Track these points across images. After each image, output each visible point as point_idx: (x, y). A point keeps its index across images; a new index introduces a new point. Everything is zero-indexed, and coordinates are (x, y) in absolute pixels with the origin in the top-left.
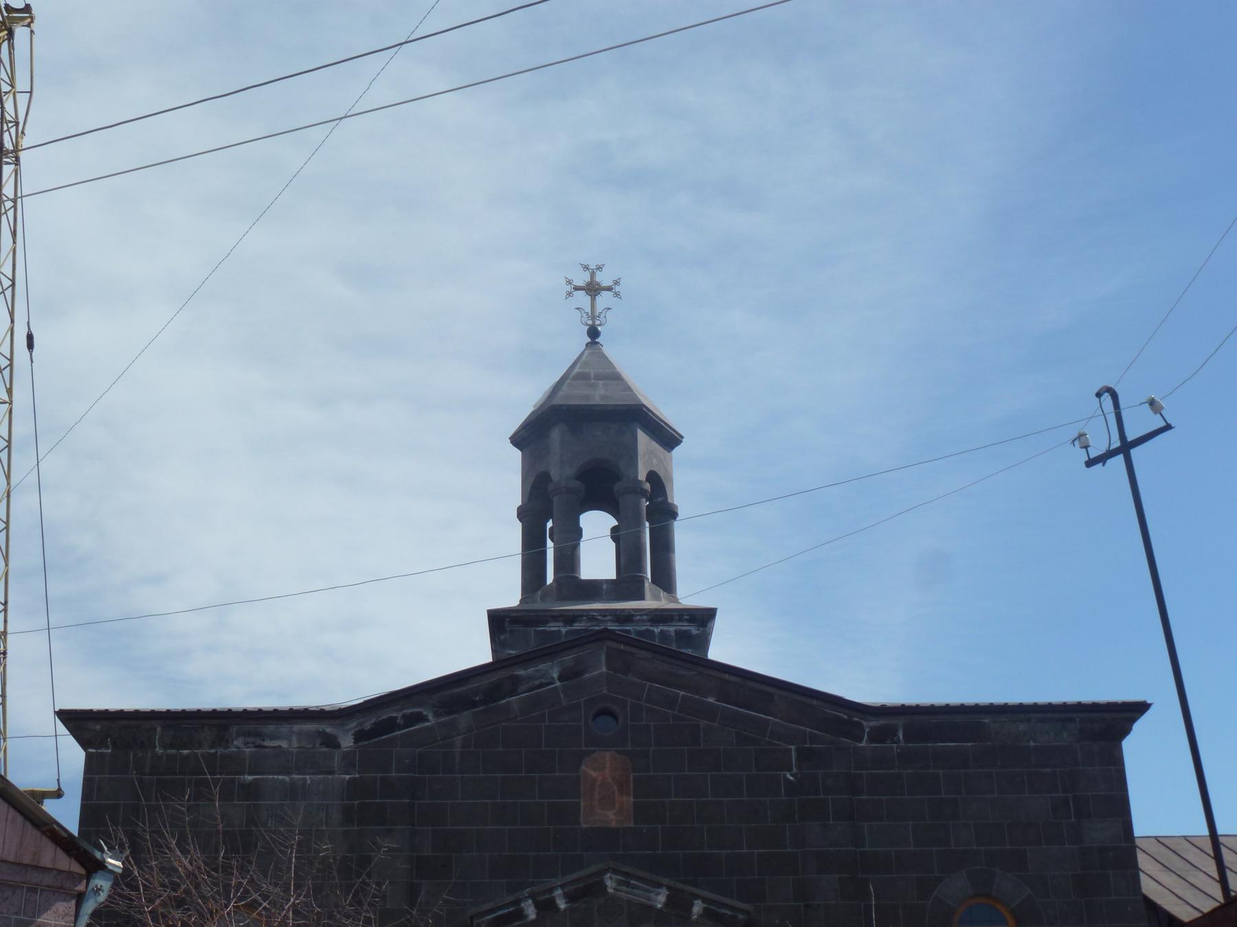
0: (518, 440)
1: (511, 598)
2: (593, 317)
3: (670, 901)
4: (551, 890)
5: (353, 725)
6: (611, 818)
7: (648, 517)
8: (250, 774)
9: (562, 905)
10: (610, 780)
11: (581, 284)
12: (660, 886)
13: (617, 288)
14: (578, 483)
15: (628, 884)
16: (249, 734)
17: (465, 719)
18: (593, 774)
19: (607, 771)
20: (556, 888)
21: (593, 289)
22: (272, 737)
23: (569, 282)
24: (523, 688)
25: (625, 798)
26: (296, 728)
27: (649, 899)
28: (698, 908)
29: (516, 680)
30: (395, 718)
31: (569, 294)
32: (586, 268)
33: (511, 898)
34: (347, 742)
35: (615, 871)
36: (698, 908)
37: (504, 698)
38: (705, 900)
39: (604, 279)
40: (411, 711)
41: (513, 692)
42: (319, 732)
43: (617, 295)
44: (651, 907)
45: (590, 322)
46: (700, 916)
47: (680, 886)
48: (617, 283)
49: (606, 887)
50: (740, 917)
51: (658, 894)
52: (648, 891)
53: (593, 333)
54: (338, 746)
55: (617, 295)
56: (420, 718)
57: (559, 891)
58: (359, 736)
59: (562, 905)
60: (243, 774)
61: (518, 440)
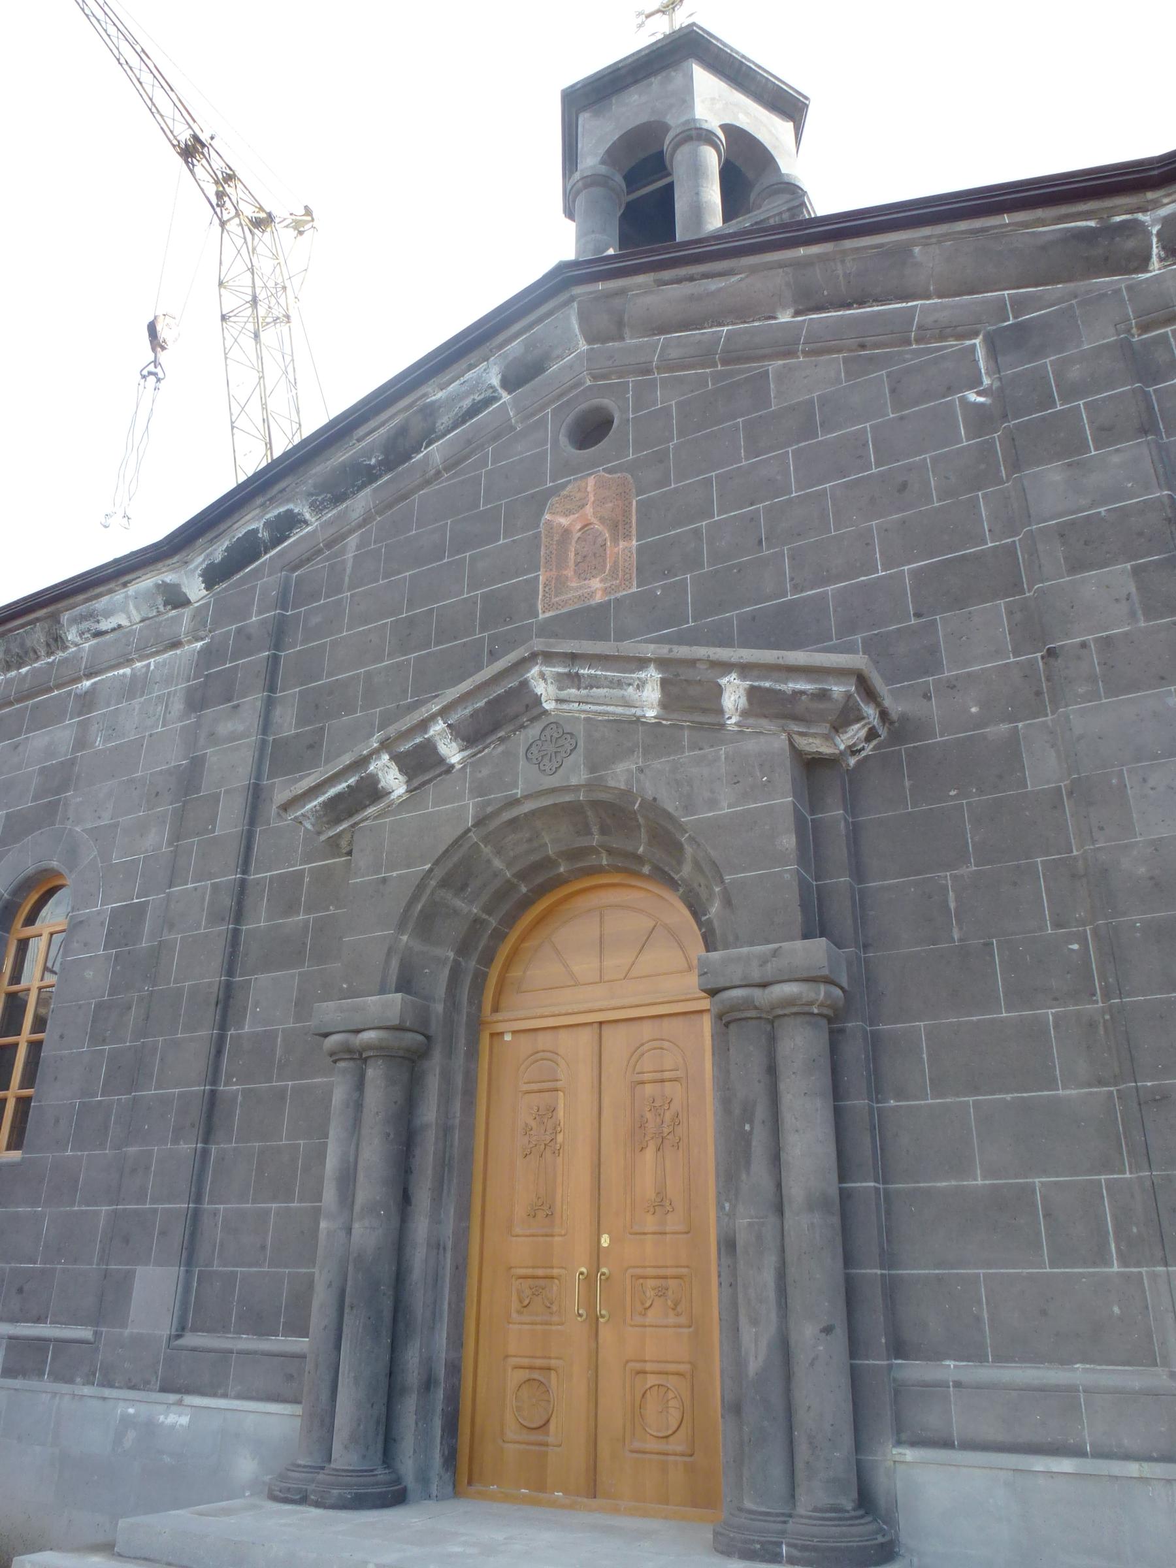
3: (672, 698)
4: (424, 725)
5: (199, 561)
6: (597, 589)
8: (89, 676)
9: (452, 753)
10: (598, 526)
12: (642, 663)
14: (603, 169)
15: (574, 680)
16: (84, 618)
17: (361, 502)
18: (564, 521)
19: (589, 509)
20: (432, 718)
22: (108, 614)
24: (444, 421)
25: (622, 544)
26: (132, 589)
27: (628, 704)
28: (733, 694)
29: (430, 412)
30: (255, 531)
31: (640, 26)
33: (347, 759)
34: (195, 590)
35: (548, 657)
36: (733, 694)
37: (418, 451)
38: (744, 669)
40: (276, 512)
41: (429, 436)
42: (158, 586)
44: (637, 721)
46: (745, 714)
47: (683, 652)
49: (537, 700)
50: (838, 689)
51: (641, 686)
52: (619, 684)
54: (186, 602)
56: (290, 522)
57: (439, 726)
58: (213, 576)
59: (452, 753)
60: (77, 680)
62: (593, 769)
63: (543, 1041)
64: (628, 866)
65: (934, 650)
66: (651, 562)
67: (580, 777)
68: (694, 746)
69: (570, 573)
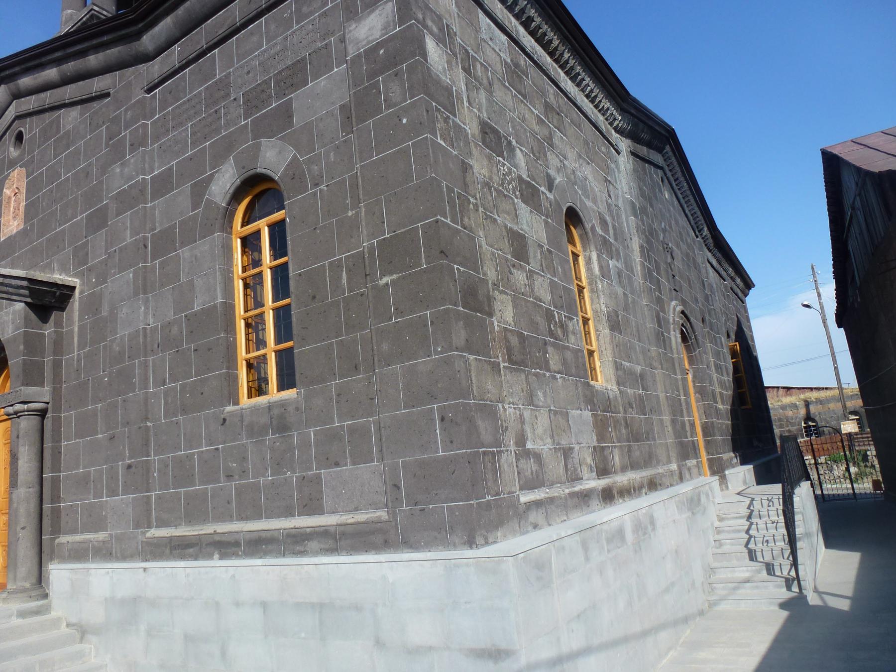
69: (11, 217)
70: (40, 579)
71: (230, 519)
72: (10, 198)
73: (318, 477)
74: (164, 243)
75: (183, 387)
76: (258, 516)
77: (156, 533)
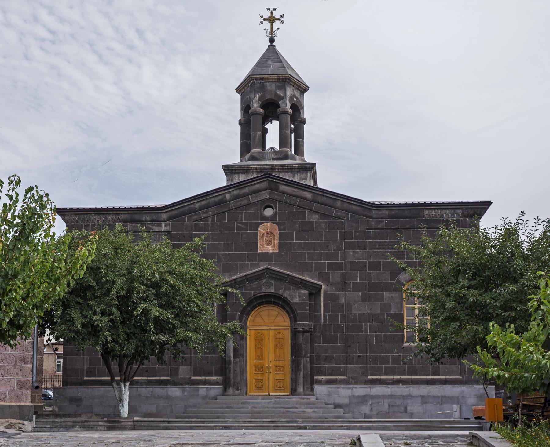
0: (238, 90)
1: (235, 159)
2: (272, 34)
6: (270, 249)
7: (295, 121)
11: (267, 17)
13: (282, 19)
14: (261, 110)
21: (272, 20)
23: (261, 17)
31: (261, 22)
32: (269, 10)
39: (276, 15)
43: (282, 22)
45: (270, 36)
48: (282, 16)
53: (272, 40)
55: (282, 22)
61: (238, 90)
62: (275, 290)
63: (260, 331)
64: (276, 304)
65: (329, 278)
66: (281, 246)
67: (273, 291)
68: (293, 290)
70: (312, 390)
71: (405, 375)
72: (264, 234)
73: (439, 367)
74: (375, 287)
75: (384, 335)
76: (417, 375)
77: (370, 377)
